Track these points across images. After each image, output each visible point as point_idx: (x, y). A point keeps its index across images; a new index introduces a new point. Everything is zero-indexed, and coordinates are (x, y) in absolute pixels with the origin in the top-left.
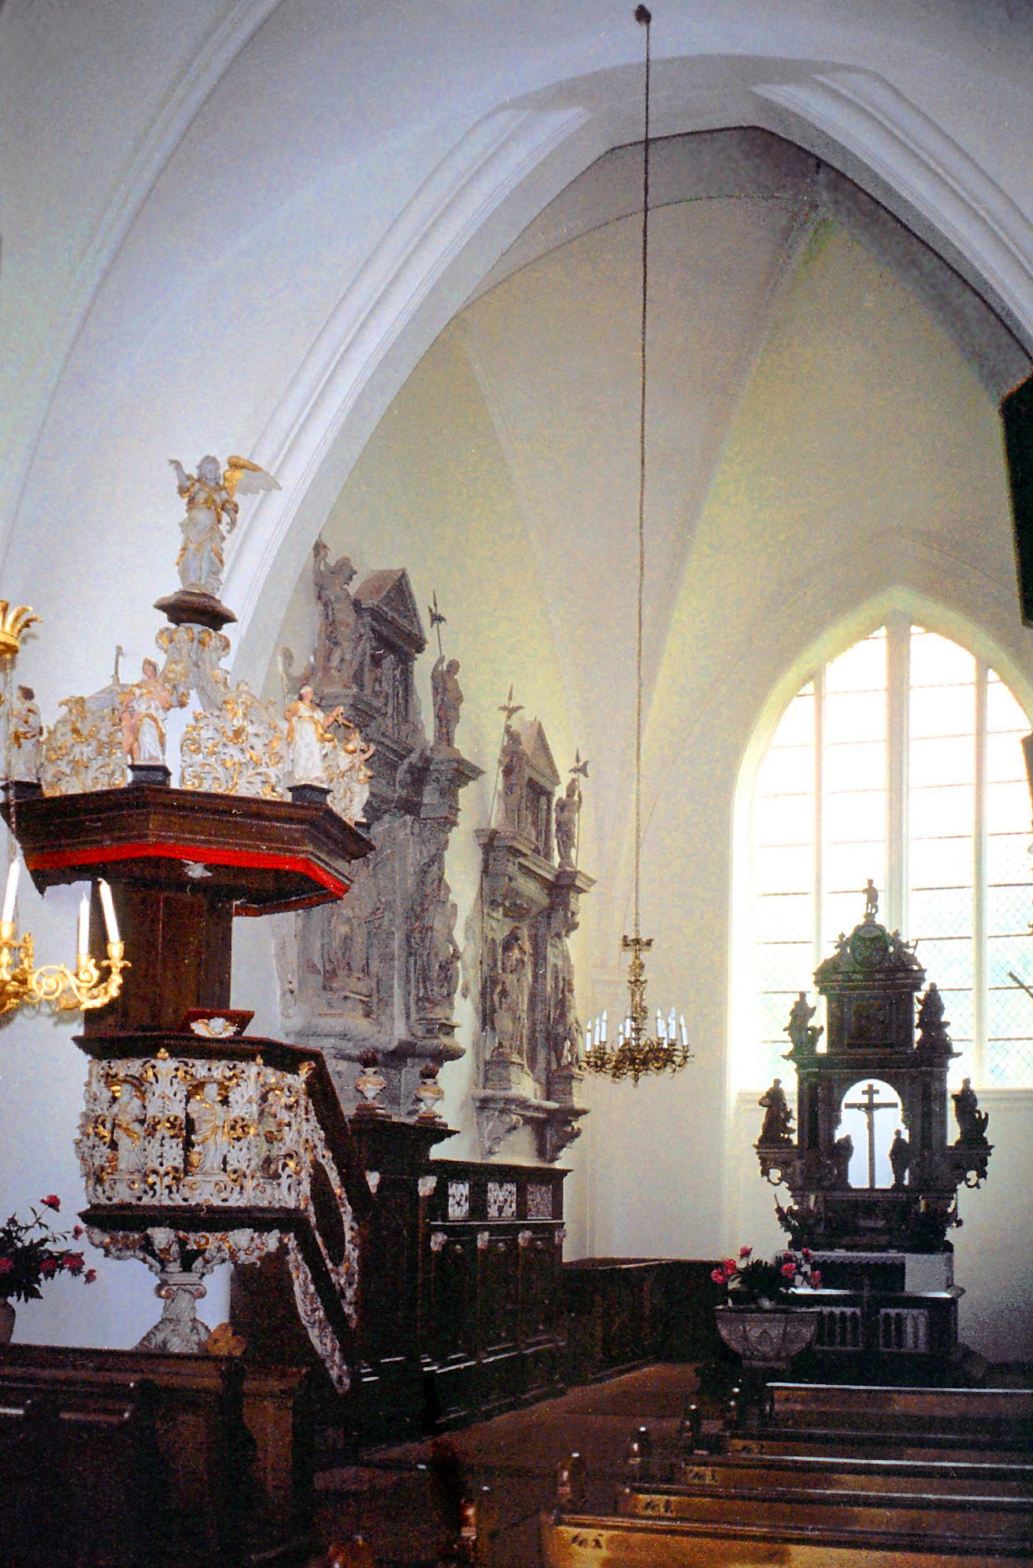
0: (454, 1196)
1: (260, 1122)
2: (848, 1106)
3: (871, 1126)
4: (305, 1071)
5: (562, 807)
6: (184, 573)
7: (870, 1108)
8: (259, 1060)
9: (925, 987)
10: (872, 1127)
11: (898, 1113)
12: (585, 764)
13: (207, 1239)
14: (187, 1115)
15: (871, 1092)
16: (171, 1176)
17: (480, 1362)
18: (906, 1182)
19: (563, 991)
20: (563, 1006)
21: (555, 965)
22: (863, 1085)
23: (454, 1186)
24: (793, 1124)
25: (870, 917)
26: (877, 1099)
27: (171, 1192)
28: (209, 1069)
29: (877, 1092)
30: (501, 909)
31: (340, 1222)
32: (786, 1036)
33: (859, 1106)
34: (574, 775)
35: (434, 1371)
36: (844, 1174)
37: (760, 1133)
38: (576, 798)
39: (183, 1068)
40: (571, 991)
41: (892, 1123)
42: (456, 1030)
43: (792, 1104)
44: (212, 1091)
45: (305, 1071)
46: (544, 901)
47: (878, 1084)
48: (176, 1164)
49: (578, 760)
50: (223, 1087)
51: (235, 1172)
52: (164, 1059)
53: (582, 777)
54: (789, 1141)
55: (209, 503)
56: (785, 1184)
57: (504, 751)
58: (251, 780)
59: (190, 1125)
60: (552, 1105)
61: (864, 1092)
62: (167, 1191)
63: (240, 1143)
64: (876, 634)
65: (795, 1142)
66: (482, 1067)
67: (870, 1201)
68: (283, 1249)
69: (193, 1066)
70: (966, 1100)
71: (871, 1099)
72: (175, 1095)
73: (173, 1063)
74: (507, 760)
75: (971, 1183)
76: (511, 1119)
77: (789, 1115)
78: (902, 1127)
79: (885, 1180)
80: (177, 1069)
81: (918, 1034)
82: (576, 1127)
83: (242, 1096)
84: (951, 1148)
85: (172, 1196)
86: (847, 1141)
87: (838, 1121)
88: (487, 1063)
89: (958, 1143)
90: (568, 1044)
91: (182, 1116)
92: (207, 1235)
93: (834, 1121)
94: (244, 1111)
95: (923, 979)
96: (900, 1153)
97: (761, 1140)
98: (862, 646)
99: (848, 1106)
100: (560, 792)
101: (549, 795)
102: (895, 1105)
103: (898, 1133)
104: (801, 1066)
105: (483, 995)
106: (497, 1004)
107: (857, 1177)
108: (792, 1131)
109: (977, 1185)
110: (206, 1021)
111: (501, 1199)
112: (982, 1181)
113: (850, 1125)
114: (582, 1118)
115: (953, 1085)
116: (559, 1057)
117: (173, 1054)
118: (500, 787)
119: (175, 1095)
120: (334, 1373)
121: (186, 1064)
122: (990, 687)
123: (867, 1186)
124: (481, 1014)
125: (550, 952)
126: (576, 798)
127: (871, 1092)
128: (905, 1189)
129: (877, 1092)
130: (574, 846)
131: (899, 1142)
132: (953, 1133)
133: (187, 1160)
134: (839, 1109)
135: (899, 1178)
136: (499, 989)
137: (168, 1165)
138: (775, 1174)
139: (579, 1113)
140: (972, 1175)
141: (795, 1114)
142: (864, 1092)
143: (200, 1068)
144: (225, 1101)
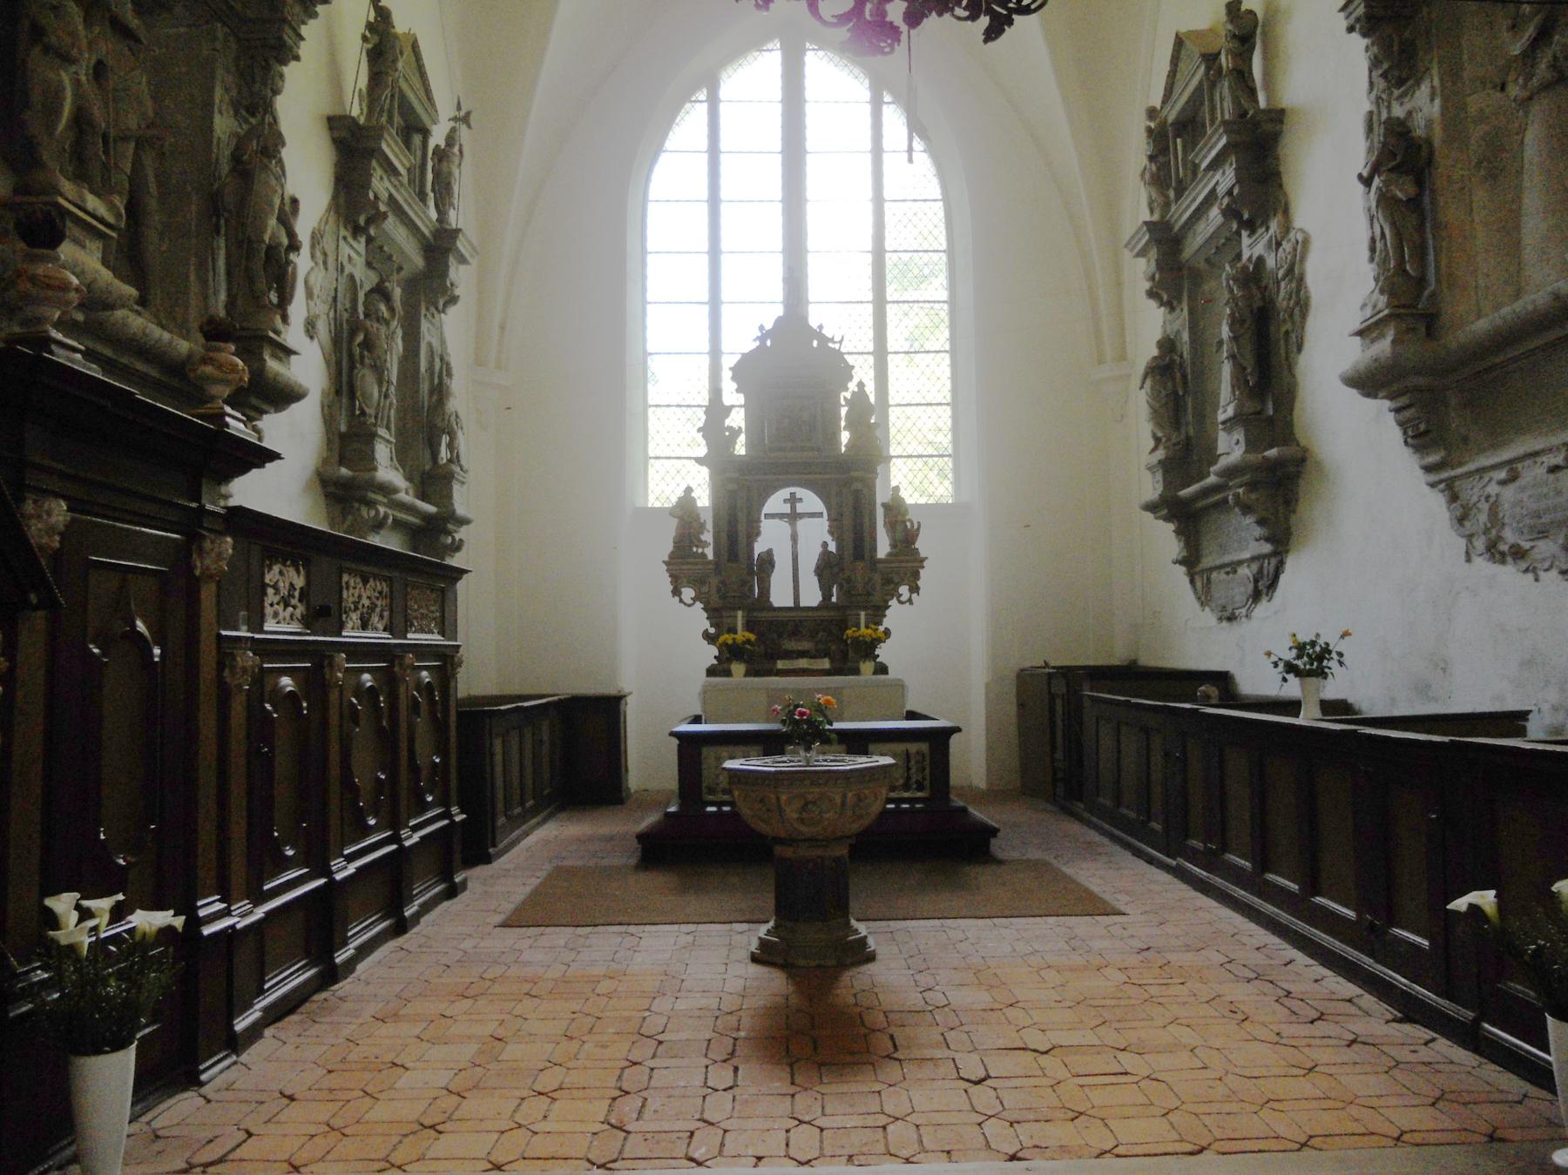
0: (275, 587)
2: (767, 516)
3: (794, 538)
5: (441, 155)
7: (793, 517)
9: (852, 386)
11: (824, 523)
12: (468, 114)
15: (793, 500)
17: (332, 881)
18: (834, 599)
19: (440, 377)
20: (440, 392)
21: (430, 345)
22: (784, 493)
23: (276, 568)
24: (708, 537)
26: (800, 508)
29: (801, 500)
30: (363, 240)
33: (781, 516)
34: (452, 124)
35: (233, 927)
36: (765, 592)
37: (670, 547)
38: (456, 150)
40: (449, 375)
41: (816, 536)
42: (293, 357)
46: (419, 261)
47: (801, 492)
49: (459, 108)
53: (464, 127)
54: (704, 555)
56: (699, 605)
57: (369, 26)
60: (431, 509)
61: (785, 501)
64: (770, 46)
65: (710, 556)
66: (337, 440)
67: (795, 622)
70: (896, 510)
71: (793, 508)
74: (376, 39)
75: (903, 599)
76: (378, 512)
77: (702, 526)
78: (829, 539)
79: (811, 596)
81: (845, 437)
82: (457, 537)
84: (881, 561)
86: (770, 553)
87: (758, 534)
88: (342, 436)
89: (890, 554)
90: (445, 439)
93: (753, 533)
95: (851, 378)
96: (828, 569)
97: (672, 556)
99: (767, 516)
100: (437, 138)
101: (426, 133)
102: (820, 515)
103: (825, 545)
105: (336, 341)
106: (357, 357)
107: (780, 596)
108: (705, 544)
109: (910, 601)
111: (366, 602)
112: (914, 596)
113: (771, 537)
114: (464, 529)
115: (881, 497)
116: (435, 455)
118: (363, 82)
122: (885, 107)
123: (791, 604)
124: (333, 368)
125: (425, 326)
126: (456, 150)
127: (793, 500)
128: (836, 607)
129: (801, 500)
130: (451, 205)
131: (825, 553)
132: (883, 548)
134: (759, 521)
135: (827, 595)
136: (360, 338)
138: (688, 593)
139: (463, 522)
140: (904, 590)
141: (709, 526)
142: (785, 501)
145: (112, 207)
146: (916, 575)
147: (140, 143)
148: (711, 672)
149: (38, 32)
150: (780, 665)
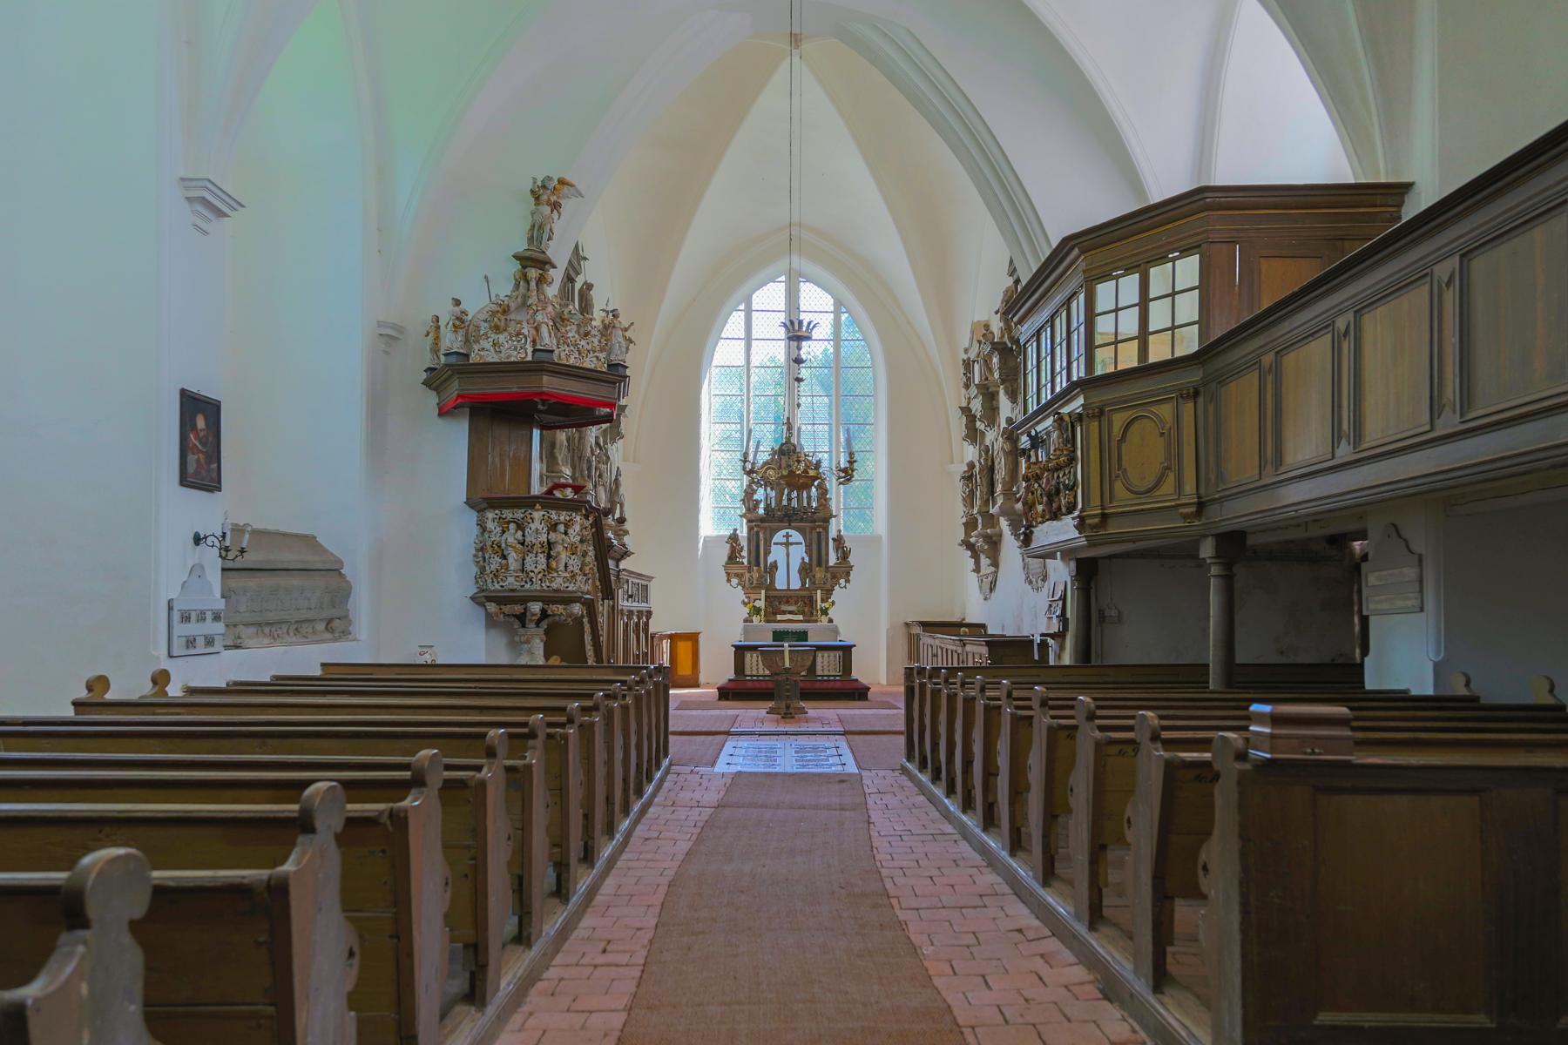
7: (787, 544)
10: (788, 556)
15: (787, 536)
22: (784, 532)
24: (745, 553)
25: (788, 439)
32: (739, 504)
36: (773, 582)
41: (799, 554)
43: (744, 543)
47: (791, 532)
50: (567, 526)
55: (549, 203)
70: (839, 541)
79: (796, 584)
96: (805, 570)
98: (771, 286)
104: (749, 521)
107: (780, 583)
113: (777, 554)
115: (833, 533)
117: (543, 508)
127: (787, 536)
133: (548, 565)
135: (803, 584)
140: (842, 581)
146: (848, 574)
148: (746, 621)
150: (779, 617)
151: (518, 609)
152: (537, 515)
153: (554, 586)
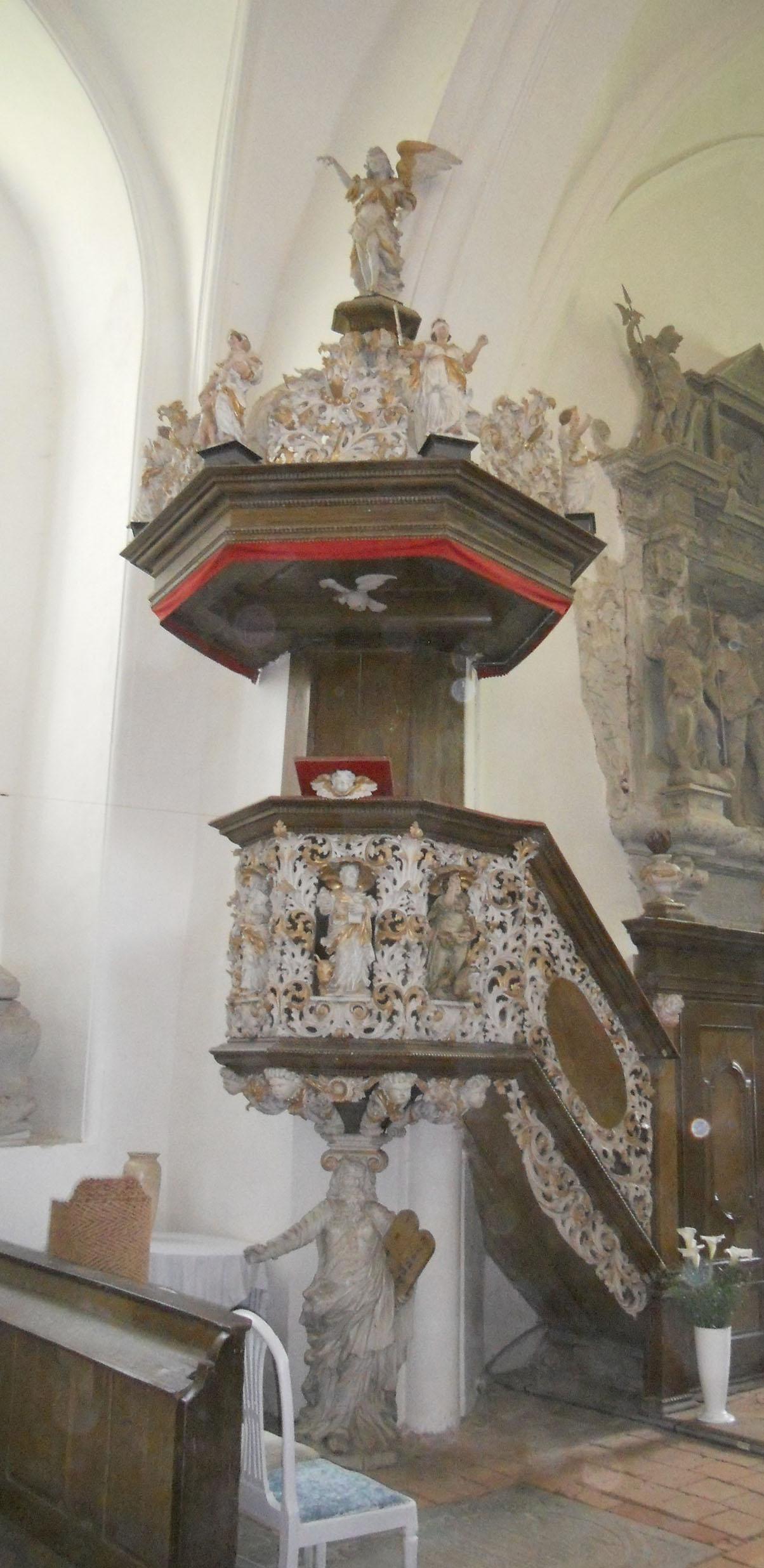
1: (433, 922)
4: (526, 851)
6: (359, 283)
8: (416, 830)
13: (344, 1086)
14: (317, 910)
16: (290, 995)
27: (290, 1018)
28: (348, 847)
31: (617, 1068)
39: (309, 845)
44: (350, 875)
45: (526, 851)
48: (300, 978)
51: (383, 989)
52: (285, 837)
58: (360, 445)
59: (322, 924)
62: (284, 1017)
63: (392, 948)
68: (497, 1103)
69: (324, 842)
72: (300, 883)
73: (300, 840)
80: (302, 848)
83: (395, 882)
85: (292, 1024)
91: (311, 912)
92: (344, 1080)
94: (400, 902)
110: (327, 777)
119: (300, 883)
120: (615, 1287)
121: (314, 841)
137: (289, 979)
143: (334, 846)
144: (373, 892)
145: (727, 779)
147: (750, 716)
149: (673, 685)
151: (353, 1088)
152: (410, 847)
153: (326, 1029)
